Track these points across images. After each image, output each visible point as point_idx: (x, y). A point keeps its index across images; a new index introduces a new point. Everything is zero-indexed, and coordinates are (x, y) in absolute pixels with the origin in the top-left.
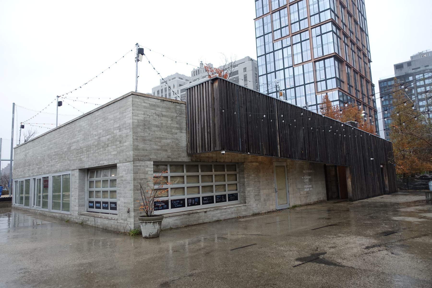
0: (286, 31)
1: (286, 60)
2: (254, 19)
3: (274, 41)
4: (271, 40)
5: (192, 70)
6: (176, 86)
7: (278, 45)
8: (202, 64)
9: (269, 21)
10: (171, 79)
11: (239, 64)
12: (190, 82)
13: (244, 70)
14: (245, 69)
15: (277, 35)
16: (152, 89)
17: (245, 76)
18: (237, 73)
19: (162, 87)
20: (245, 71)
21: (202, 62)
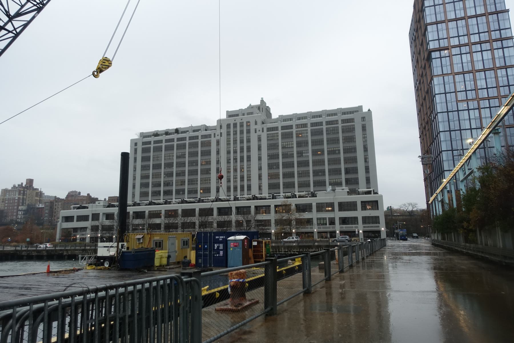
0: (471, 95)
1: (473, 122)
3: (457, 101)
4: (454, 99)
6: (259, 122)
7: (463, 106)
9: (452, 80)
10: (246, 114)
13: (363, 119)
15: (461, 96)
16: (217, 121)
18: (352, 120)
19: (235, 120)
20: (363, 120)
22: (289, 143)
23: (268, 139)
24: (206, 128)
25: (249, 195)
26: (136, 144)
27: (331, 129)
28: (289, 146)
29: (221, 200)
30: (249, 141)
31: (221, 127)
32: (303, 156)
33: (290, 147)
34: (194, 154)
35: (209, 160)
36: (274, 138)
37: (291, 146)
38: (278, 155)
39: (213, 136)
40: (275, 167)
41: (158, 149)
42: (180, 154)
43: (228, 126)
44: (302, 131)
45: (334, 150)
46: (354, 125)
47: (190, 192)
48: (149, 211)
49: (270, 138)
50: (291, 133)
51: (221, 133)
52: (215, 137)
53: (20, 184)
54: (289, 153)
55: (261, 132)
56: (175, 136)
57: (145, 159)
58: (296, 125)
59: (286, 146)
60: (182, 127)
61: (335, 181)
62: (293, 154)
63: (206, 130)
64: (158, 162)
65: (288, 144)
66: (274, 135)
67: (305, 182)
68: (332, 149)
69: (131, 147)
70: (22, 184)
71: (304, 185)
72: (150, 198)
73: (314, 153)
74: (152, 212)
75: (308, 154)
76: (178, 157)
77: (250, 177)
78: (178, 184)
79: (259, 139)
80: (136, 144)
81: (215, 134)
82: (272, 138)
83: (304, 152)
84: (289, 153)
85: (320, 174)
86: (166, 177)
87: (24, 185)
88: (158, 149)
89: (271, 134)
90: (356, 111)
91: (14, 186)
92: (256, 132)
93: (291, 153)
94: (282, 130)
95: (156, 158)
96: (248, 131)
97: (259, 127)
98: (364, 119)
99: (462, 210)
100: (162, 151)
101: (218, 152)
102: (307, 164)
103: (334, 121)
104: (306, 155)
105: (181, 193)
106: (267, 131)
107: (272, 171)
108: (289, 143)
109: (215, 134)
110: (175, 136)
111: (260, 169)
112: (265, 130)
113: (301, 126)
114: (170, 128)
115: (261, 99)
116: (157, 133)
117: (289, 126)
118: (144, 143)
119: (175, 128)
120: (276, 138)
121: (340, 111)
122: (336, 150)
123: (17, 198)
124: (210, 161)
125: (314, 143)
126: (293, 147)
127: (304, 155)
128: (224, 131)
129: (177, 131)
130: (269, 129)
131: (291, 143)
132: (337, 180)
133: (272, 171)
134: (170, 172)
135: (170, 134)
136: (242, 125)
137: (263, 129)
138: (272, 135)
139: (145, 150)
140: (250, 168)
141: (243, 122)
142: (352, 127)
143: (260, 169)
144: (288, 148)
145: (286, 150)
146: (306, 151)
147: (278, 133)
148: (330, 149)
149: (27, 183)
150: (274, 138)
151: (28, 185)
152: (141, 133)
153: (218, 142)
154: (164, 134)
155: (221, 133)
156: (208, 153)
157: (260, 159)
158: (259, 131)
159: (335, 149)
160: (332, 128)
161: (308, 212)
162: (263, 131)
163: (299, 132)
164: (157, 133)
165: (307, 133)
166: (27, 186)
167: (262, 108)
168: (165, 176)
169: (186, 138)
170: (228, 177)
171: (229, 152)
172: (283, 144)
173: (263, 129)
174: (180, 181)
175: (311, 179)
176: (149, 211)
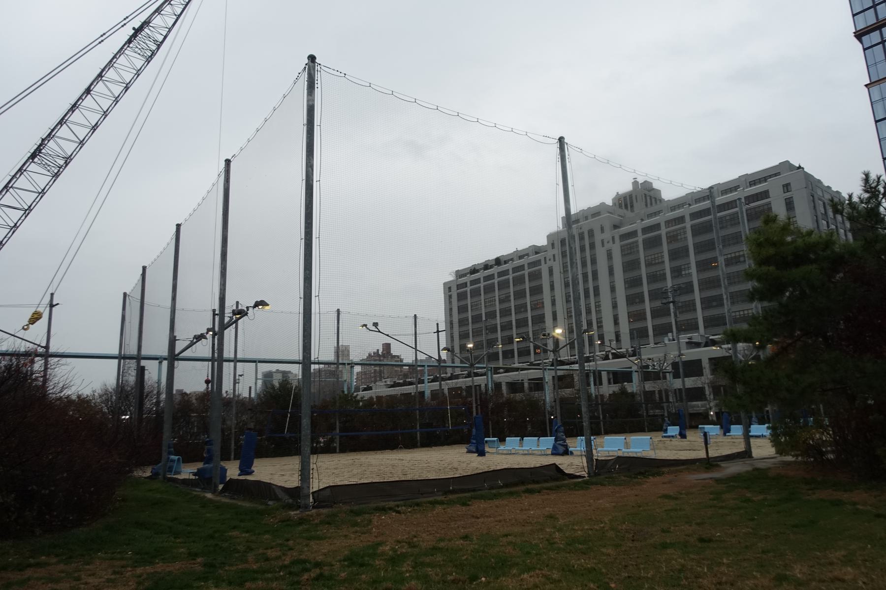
2: (866, 86)
5: (614, 195)
8: (635, 183)
10: (590, 217)
11: (770, 176)
12: (642, 220)
13: (785, 188)
14: (787, 187)
17: (788, 201)
18: (765, 194)
20: (786, 191)
21: (638, 180)
22: (656, 256)
23: (623, 253)
24: (537, 250)
25: (603, 351)
26: (450, 288)
27: (728, 218)
28: (657, 261)
29: (562, 363)
30: (594, 261)
31: (553, 245)
32: (682, 275)
33: (659, 263)
34: (520, 295)
35: (541, 301)
36: (632, 251)
37: (660, 260)
38: (640, 279)
39: (543, 262)
40: (637, 300)
41: (476, 293)
43: (563, 242)
44: (676, 230)
45: (735, 257)
46: (770, 203)
47: (520, 354)
48: (431, 391)
49: (626, 253)
50: (659, 238)
51: (554, 256)
52: (546, 263)
53: (376, 351)
54: (658, 273)
56: (495, 270)
57: (462, 309)
58: (666, 222)
59: (653, 262)
60: (505, 254)
61: (744, 314)
62: (665, 274)
63: (537, 253)
64: (491, 309)
65: (655, 260)
66: (632, 245)
67: (689, 322)
68: (733, 255)
69: (445, 293)
70: (378, 350)
71: (524, 353)
72: (532, 358)
73: (703, 266)
74: (435, 392)
75: (690, 271)
76: (501, 301)
77: (601, 322)
79: (610, 256)
80: (450, 288)
81: (545, 258)
82: (629, 252)
83: (683, 267)
84: (658, 273)
85: (714, 304)
86: (490, 333)
87: (380, 352)
88: (476, 293)
89: (627, 245)
90: (776, 175)
91: (370, 355)
92: (603, 245)
93: (662, 272)
94: (643, 234)
95: (475, 306)
96: (592, 246)
97: (607, 235)
98: (789, 187)
99: (180, 433)
100: (481, 295)
101: (552, 288)
102: (689, 288)
103: (731, 202)
104: (687, 272)
105: (510, 356)
106: (621, 241)
107: (636, 308)
108: (656, 256)
109: (545, 258)
110: (495, 270)
111: (615, 306)
113: (674, 222)
114: (490, 259)
115: (633, 181)
116: (475, 269)
117: (704, 210)
118: (459, 286)
119: (495, 257)
120: (635, 250)
121: (746, 180)
122: (740, 256)
123: (373, 371)
125: (700, 248)
126: (663, 262)
127: (683, 273)
128: (557, 251)
129: (498, 261)
130: (624, 237)
131: (660, 255)
132: (746, 312)
133: (636, 308)
135: (491, 267)
136: (582, 238)
137: (613, 238)
138: (629, 246)
139: (462, 297)
140: (599, 306)
141: (583, 233)
142: (766, 207)
143: (615, 306)
144: (655, 264)
145: (653, 269)
146: (686, 266)
147: (637, 242)
148: (729, 256)
149: (383, 351)
150: (632, 251)
151: (385, 352)
152: (457, 272)
154: (468, 273)
156: (537, 290)
157: (613, 289)
158: (608, 242)
159: (737, 254)
160: (730, 215)
161: (628, 383)
162: (614, 243)
163: (672, 234)
164: (475, 269)
165: (685, 233)
166: (384, 354)
167: (636, 196)
169: (480, 279)
170: (570, 326)
172: (647, 259)
173: (613, 238)
175: (700, 315)
176: (431, 391)
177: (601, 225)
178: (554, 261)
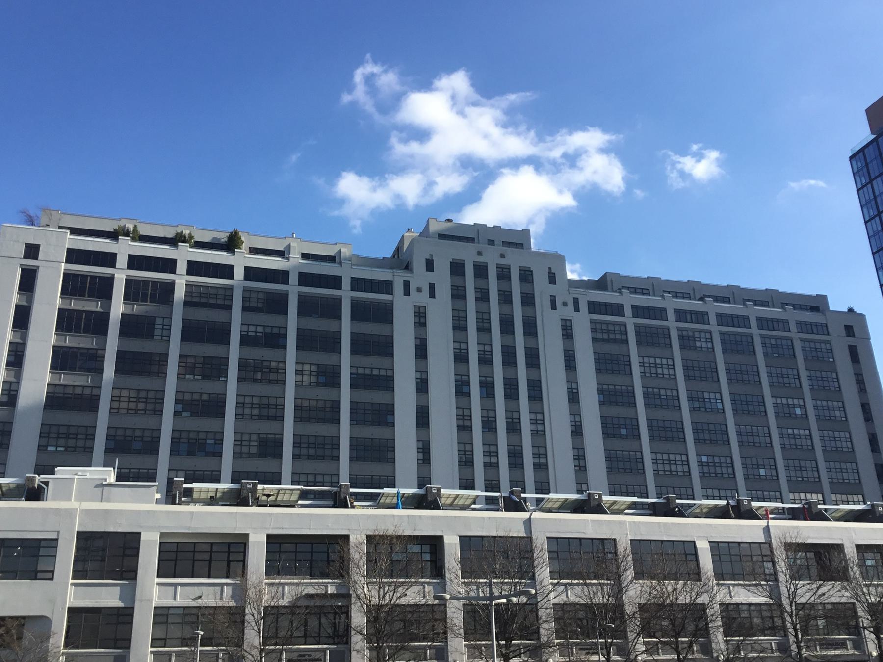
39: (398, 288)
42: (260, 329)
44: (694, 331)
51: (432, 287)
52: (407, 292)
54: (663, 392)
55: (568, 312)
66: (611, 327)
78: (245, 449)
81: (407, 285)
92: (554, 307)
96: (528, 300)
109: (407, 285)
112: (584, 307)
124: (392, 378)
134: (205, 397)
141: (508, 268)
153: (421, 317)
155: (432, 287)
162: (577, 309)
168: (180, 407)
171: (461, 358)
173: (576, 301)
174: (254, 437)
177: (550, 268)
178: (432, 295)
